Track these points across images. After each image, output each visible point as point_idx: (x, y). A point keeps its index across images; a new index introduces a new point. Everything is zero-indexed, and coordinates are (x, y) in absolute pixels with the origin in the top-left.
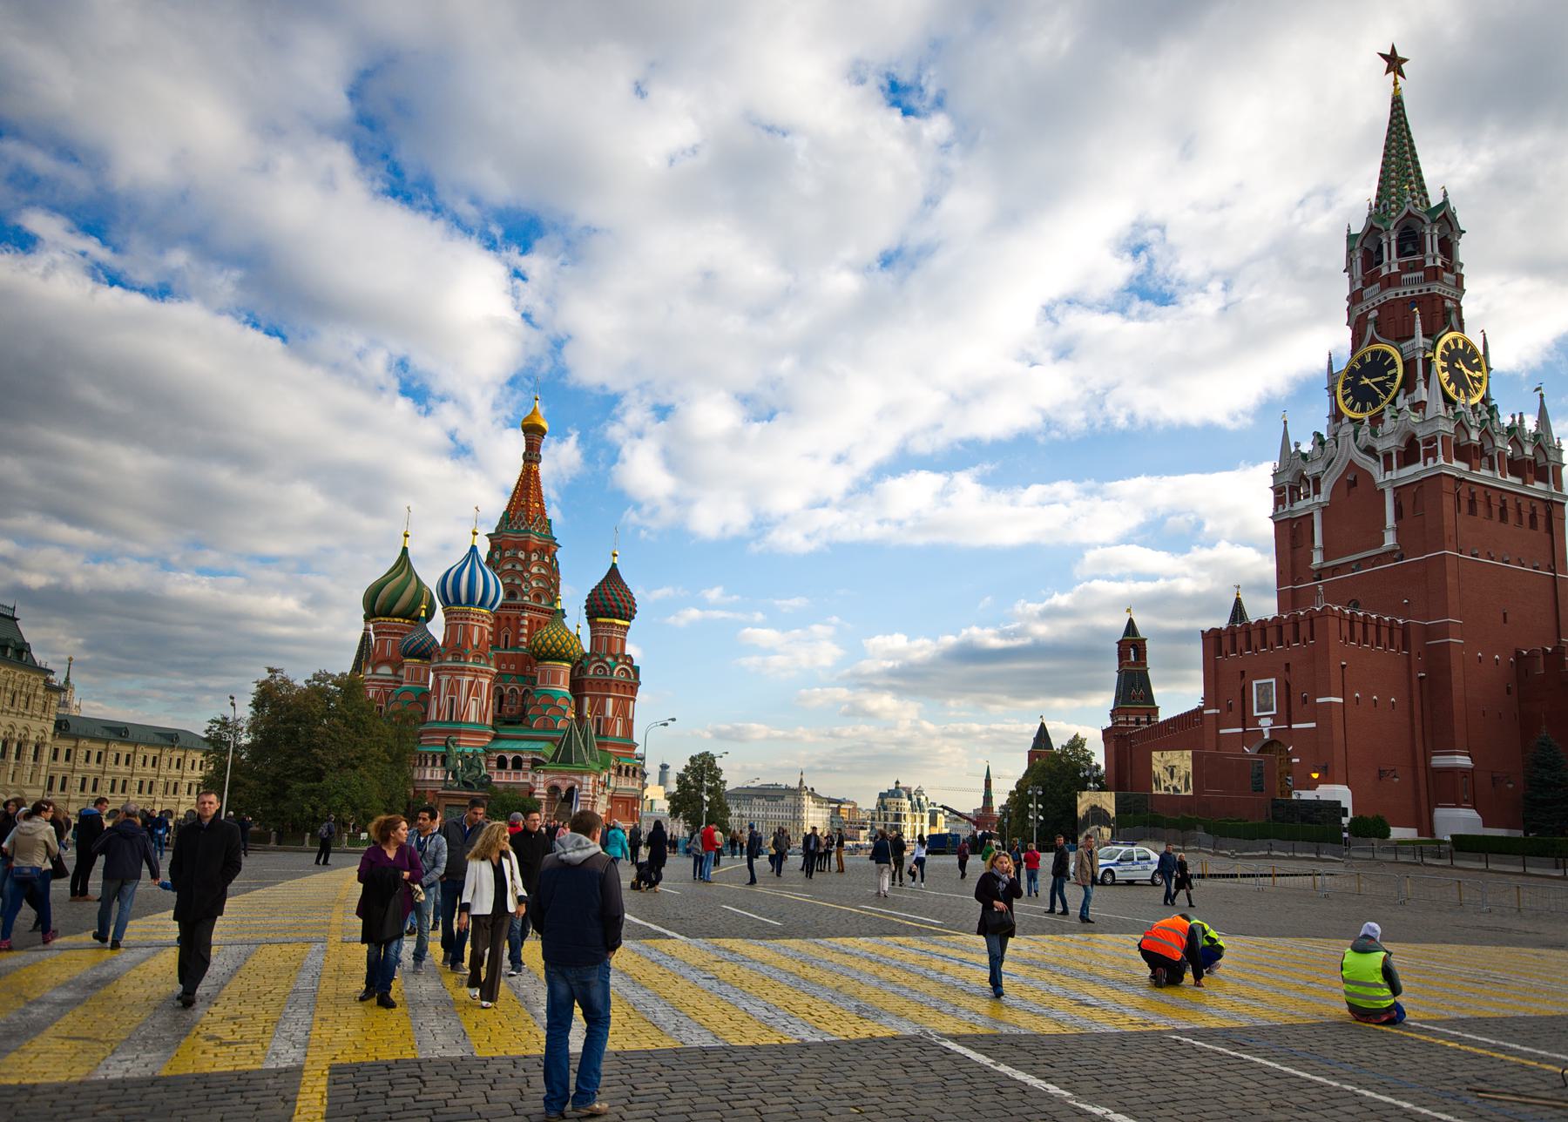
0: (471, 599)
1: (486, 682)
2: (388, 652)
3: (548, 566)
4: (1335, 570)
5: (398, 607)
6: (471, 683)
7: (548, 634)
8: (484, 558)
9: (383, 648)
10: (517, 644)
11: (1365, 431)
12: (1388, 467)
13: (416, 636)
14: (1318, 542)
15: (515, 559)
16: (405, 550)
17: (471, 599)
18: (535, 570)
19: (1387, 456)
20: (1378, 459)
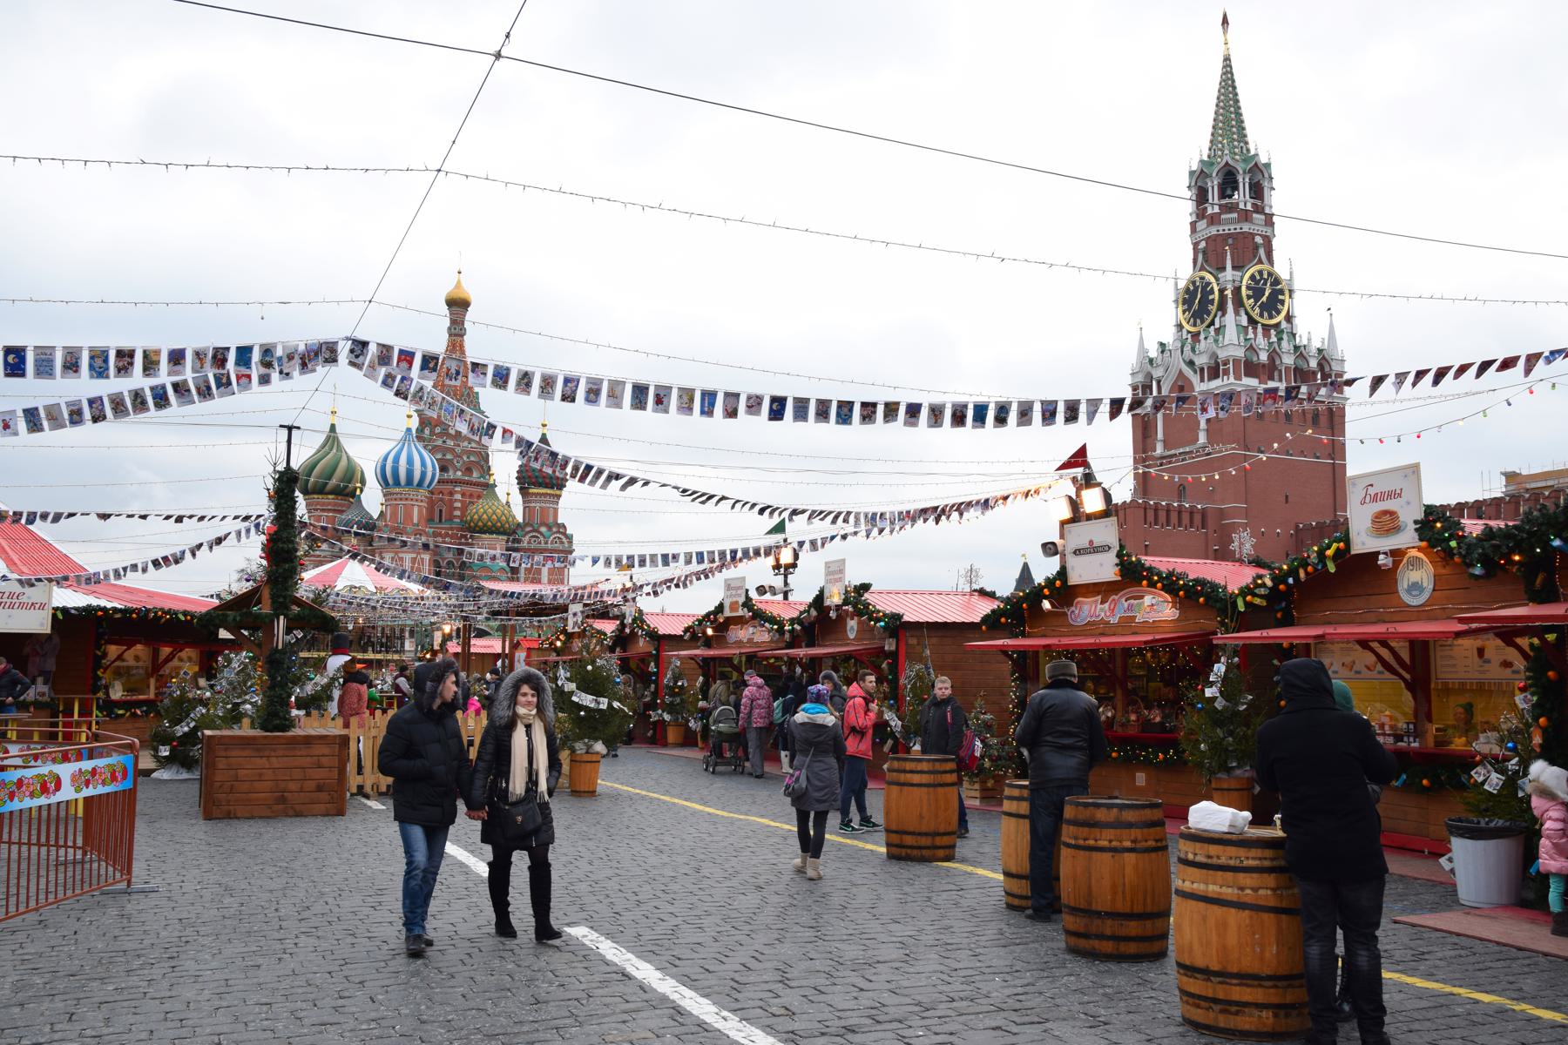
7: (481, 510)
10: (451, 518)
11: (1187, 348)
12: (1202, 380)
14: (1160, 435)
16: (333, 427)
17: (409, 481)
19: (1202, 370)
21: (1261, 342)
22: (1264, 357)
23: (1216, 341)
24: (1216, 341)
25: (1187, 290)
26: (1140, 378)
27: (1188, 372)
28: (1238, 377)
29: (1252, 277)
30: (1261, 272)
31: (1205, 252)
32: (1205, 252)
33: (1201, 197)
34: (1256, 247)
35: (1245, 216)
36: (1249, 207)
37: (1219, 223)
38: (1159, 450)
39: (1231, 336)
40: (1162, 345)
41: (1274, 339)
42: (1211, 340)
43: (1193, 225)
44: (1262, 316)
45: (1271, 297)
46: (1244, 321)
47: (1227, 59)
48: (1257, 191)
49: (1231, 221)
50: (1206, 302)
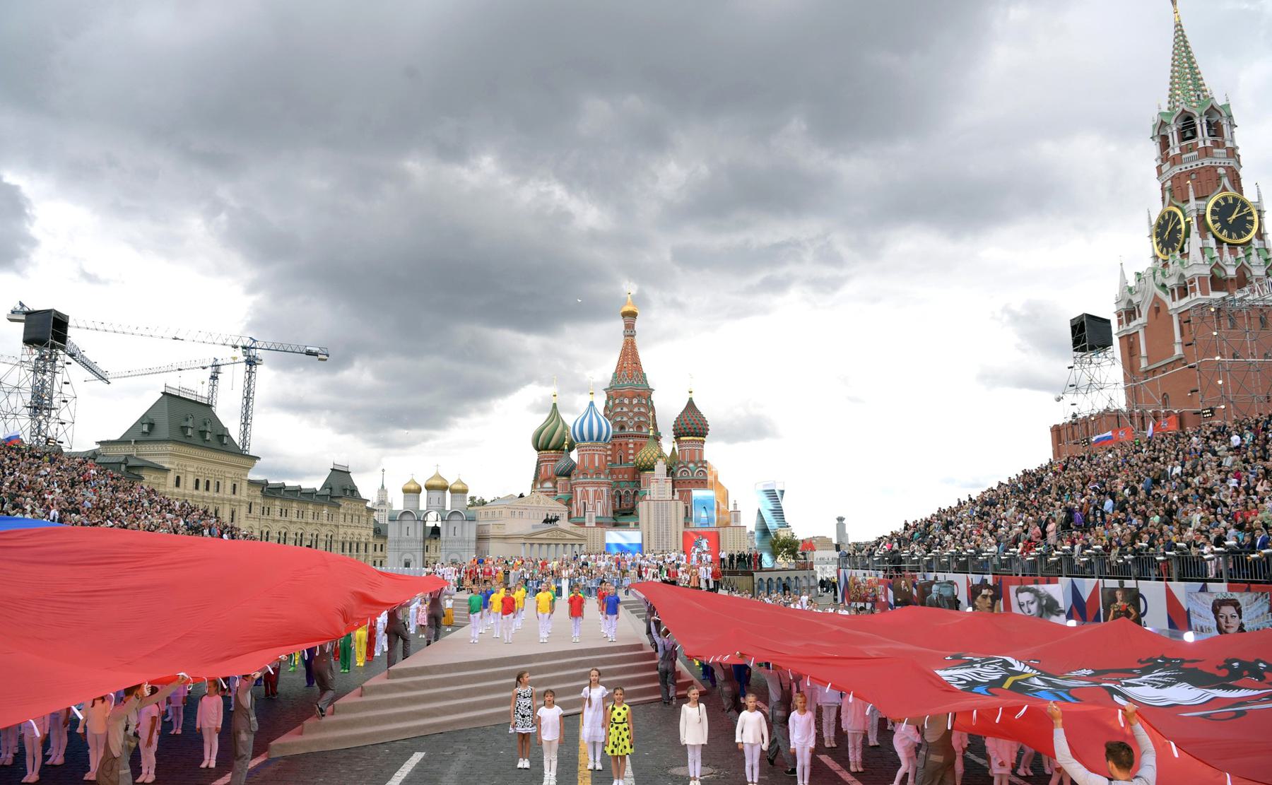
0: (591, 438)
1: (604, 489)
2: (549, 472)
3: (646, 406)
4: (1154, 371)
5: (551, 445)
6: (595, 491)
7: (646, 454)
8: (601, 410)
9: (546, 471)
11: (1158, 274)
13: (562, 464)
14: (1143, 352)
15: (622, 404)
17: (591, 438)
18: (636, 410)
19: (1173, 290)
20: (1167, 293)
21: (1228, 258)
22: (1231, 272)
23: (1182, 263)
24: (1182, 263)
25: (1159, 225)
26: (1123, 305)
27: (1161, 294)
28: (1205, 292)
29: (1217, 204)
30: (1225, 199)
31: (1171, 190)
32: (1171, 190)
33: (1164, 143)
34: (1219, 178)
35: (1206, 152)
36: (1208, 144)
37: (1181, 163)
38: (1144, 364)
39: (1198, 254)
40: (1138, 274)
41: (1241, 255)
42: (1177, 264)
43: (1159, 168)
44: (1230, 236)
45: (1236, 220)
46: (1212, 242)
47: (1179, 27)
48: (1215, 129)
49: (1190, 160)
50: (1175, 231)
